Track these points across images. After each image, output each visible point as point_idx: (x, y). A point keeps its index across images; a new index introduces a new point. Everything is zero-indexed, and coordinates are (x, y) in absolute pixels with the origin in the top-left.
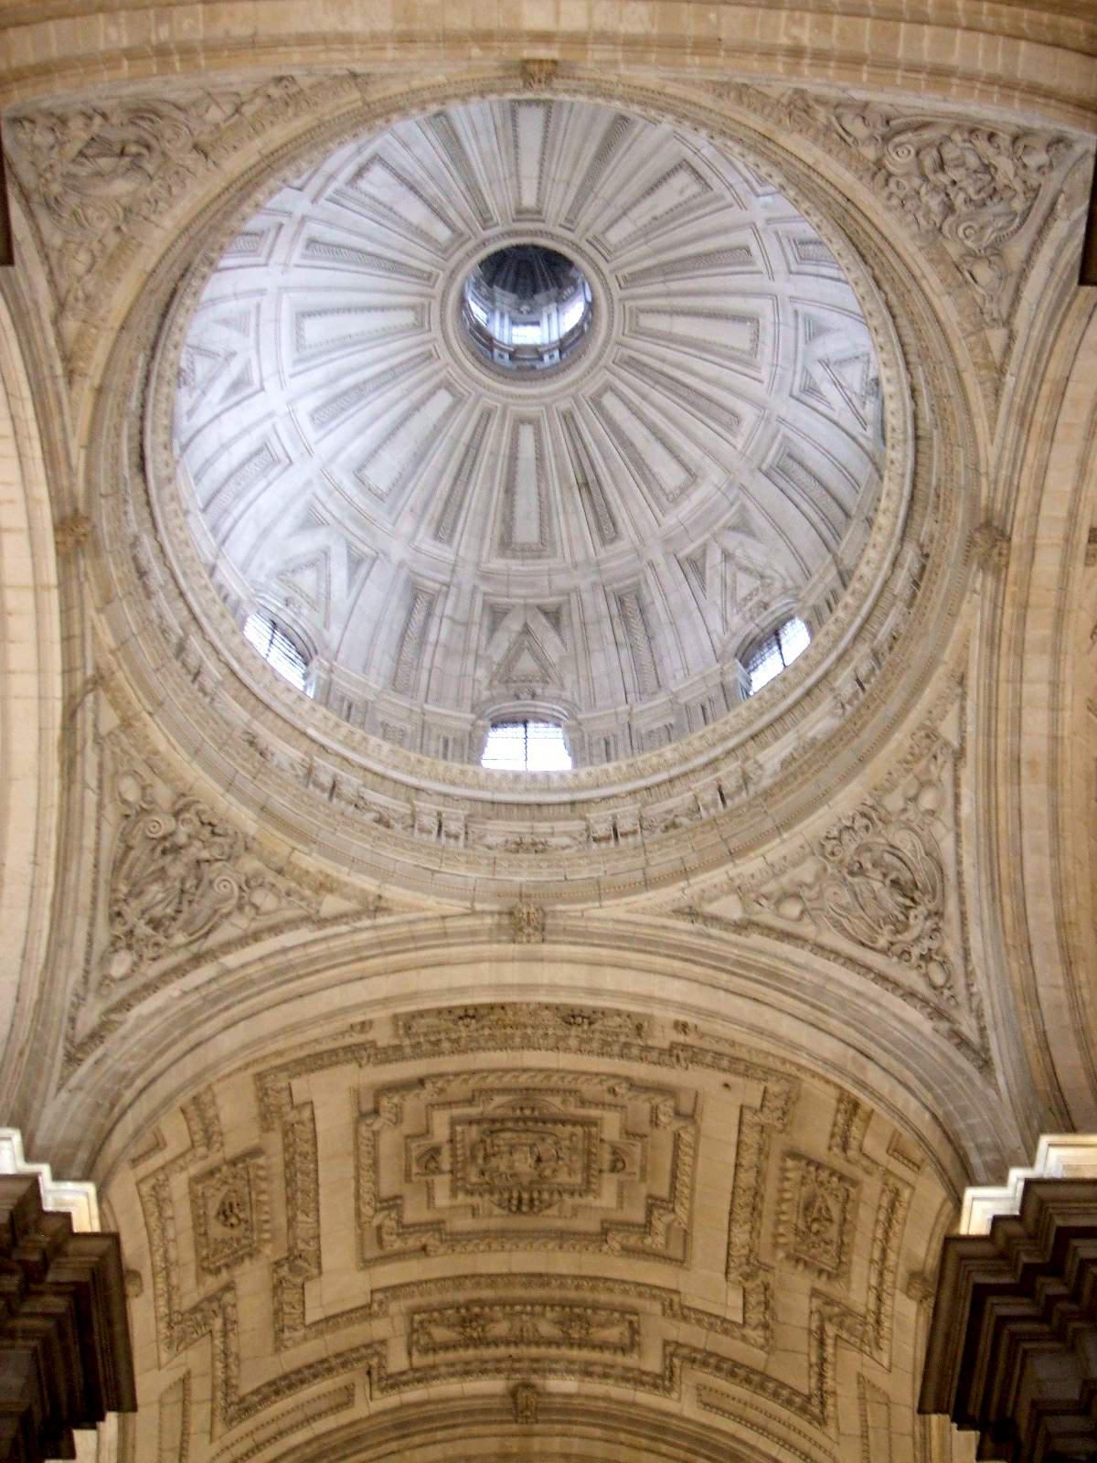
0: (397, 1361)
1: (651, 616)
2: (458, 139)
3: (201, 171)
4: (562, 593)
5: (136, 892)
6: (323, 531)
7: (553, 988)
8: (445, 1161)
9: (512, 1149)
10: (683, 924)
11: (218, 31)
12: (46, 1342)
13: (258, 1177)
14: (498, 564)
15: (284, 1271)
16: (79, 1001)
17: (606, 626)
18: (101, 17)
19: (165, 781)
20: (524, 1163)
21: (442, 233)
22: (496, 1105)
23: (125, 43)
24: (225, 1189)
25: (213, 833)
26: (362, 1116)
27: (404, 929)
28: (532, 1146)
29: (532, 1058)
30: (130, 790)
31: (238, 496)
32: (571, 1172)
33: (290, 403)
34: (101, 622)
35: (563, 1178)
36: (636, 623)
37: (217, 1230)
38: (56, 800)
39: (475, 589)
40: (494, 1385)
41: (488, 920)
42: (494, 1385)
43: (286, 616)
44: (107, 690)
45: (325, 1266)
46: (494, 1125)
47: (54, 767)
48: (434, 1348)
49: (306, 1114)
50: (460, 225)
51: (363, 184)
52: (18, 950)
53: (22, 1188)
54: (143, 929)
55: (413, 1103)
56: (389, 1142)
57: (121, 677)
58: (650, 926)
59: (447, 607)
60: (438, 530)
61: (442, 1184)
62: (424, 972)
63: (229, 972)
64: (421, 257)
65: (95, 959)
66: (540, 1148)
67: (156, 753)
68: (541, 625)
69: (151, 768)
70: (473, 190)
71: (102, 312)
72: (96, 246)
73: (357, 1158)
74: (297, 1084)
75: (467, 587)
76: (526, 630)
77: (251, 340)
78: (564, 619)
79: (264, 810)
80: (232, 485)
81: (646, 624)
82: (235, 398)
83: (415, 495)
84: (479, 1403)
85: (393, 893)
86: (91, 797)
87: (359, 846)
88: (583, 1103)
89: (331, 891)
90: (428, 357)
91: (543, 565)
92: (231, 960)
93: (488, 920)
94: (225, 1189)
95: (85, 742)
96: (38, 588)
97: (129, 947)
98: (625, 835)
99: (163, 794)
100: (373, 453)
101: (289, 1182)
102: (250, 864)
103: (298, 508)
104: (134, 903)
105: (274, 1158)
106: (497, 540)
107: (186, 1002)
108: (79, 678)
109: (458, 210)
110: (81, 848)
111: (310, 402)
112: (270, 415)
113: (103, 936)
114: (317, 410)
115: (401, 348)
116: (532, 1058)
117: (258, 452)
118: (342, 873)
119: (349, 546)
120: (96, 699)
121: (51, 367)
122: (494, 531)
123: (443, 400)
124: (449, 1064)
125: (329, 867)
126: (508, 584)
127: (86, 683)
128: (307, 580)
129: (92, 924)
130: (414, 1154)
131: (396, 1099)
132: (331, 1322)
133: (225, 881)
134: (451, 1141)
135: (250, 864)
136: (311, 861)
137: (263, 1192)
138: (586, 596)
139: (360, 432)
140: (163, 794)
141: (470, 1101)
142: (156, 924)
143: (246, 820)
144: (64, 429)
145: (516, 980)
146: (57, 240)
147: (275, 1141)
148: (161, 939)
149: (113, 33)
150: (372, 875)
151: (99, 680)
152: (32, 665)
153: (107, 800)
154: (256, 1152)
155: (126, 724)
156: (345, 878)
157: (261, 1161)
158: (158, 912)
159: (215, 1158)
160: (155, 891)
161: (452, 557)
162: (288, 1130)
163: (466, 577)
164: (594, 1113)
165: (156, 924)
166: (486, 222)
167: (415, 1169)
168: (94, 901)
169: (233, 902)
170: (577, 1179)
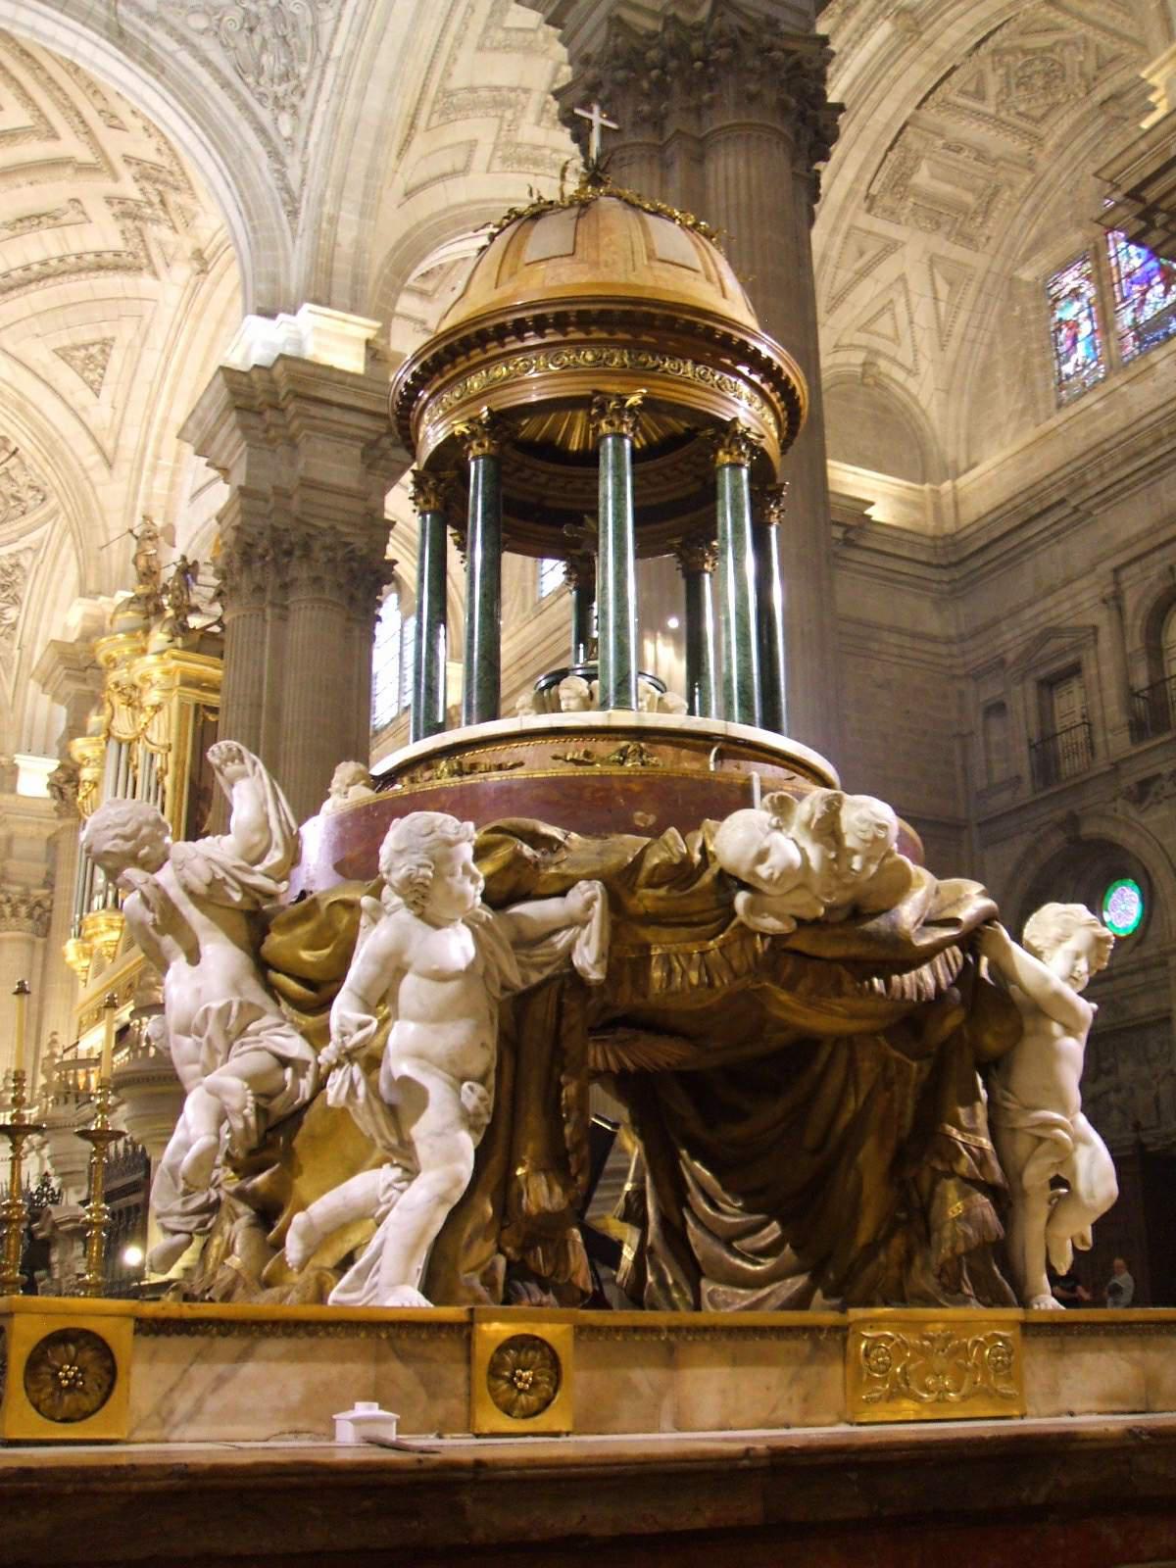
5: (260, 71)
40: (883, 31)
42: (883, 31)
53: (221, 378)
54: (280, 90)
84: (884, 52)
95: (147, 35)
142: (285, 77)
160: (267, 60)
165: (285, 77)
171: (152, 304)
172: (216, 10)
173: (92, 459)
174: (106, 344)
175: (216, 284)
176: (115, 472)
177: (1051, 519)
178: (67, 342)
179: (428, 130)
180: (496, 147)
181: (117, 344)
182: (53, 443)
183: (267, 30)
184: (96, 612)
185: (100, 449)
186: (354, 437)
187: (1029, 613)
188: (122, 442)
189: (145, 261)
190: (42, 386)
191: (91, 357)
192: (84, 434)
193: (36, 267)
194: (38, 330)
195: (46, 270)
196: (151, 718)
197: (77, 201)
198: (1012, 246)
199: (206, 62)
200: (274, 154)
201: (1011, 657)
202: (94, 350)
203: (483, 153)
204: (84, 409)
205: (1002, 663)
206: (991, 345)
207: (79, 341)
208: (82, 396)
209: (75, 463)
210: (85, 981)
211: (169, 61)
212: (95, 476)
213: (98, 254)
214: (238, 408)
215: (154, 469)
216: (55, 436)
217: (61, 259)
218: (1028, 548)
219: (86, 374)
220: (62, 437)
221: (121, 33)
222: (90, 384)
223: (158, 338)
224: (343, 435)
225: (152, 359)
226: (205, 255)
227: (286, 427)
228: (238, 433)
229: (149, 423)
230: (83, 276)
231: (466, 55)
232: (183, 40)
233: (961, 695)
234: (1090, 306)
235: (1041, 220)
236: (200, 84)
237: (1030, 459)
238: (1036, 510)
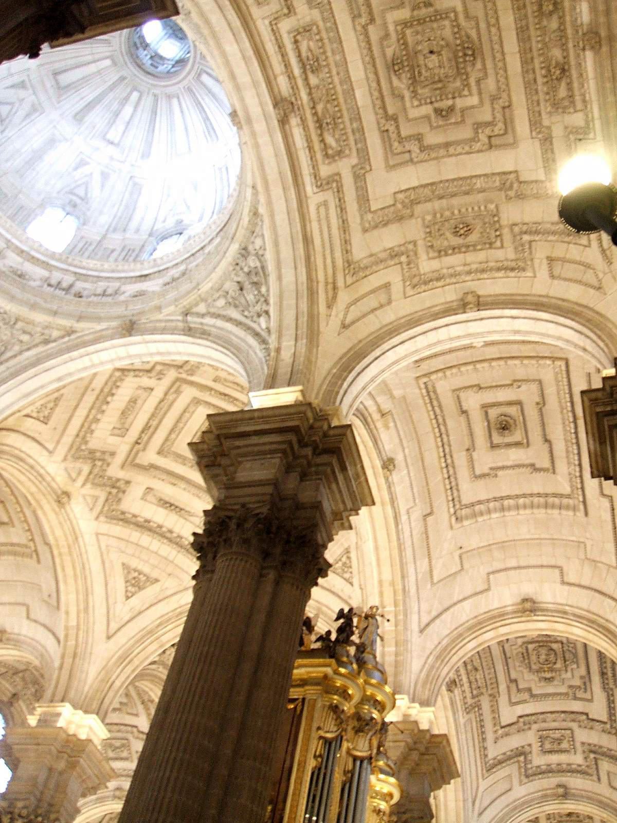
2: (89, 104)
7: (261, 104)
13: (442, 216)
15: (512, 193)
21: (135, 95)
28: (425, 57)
32: (442, 28)
34: (165, 311)
35: (448, 33)
37: (473, 237)
44: (191, 308)
45: (511, 169)
46: (414, 81)
48: (571, 96)
50: (128, 90)
51: (116, 141)
56: (433, 138)
61: (460, 103)
64: (147, 102)
66: (426, 51)
67: (212, 288)
69: (219, 289)
70: (112, 88)
73: (443, 157)
86: (219, 323)
88: (387, 36)
89: (257, 209)
90: (189, 90)
101: (454, 195)
109: (120, 91)
115: (187, 101)
116: (357, 71)
121: (65, 343)
123: (205, 78)
124: (369, 119)
125: (246, 211)
130: (441, 123)
134: (431, 103)
137: (453, 213)
146: (17, 348)
147: (418, 209)
153: (224, 313)
155: (203, 300)
156: (249, 204)
162: (415, 202)
166: (122, 79)
167: (453, 120)
179: (347, 287)
180: (404, 281)
186: (272, 452)
190: (327, 593)
199: (230, 320)
203: (397, 287)
221: (190, 329)
224: (264, 453)
231: (356, 237)
232: (218, 316)
236: (227, 331)
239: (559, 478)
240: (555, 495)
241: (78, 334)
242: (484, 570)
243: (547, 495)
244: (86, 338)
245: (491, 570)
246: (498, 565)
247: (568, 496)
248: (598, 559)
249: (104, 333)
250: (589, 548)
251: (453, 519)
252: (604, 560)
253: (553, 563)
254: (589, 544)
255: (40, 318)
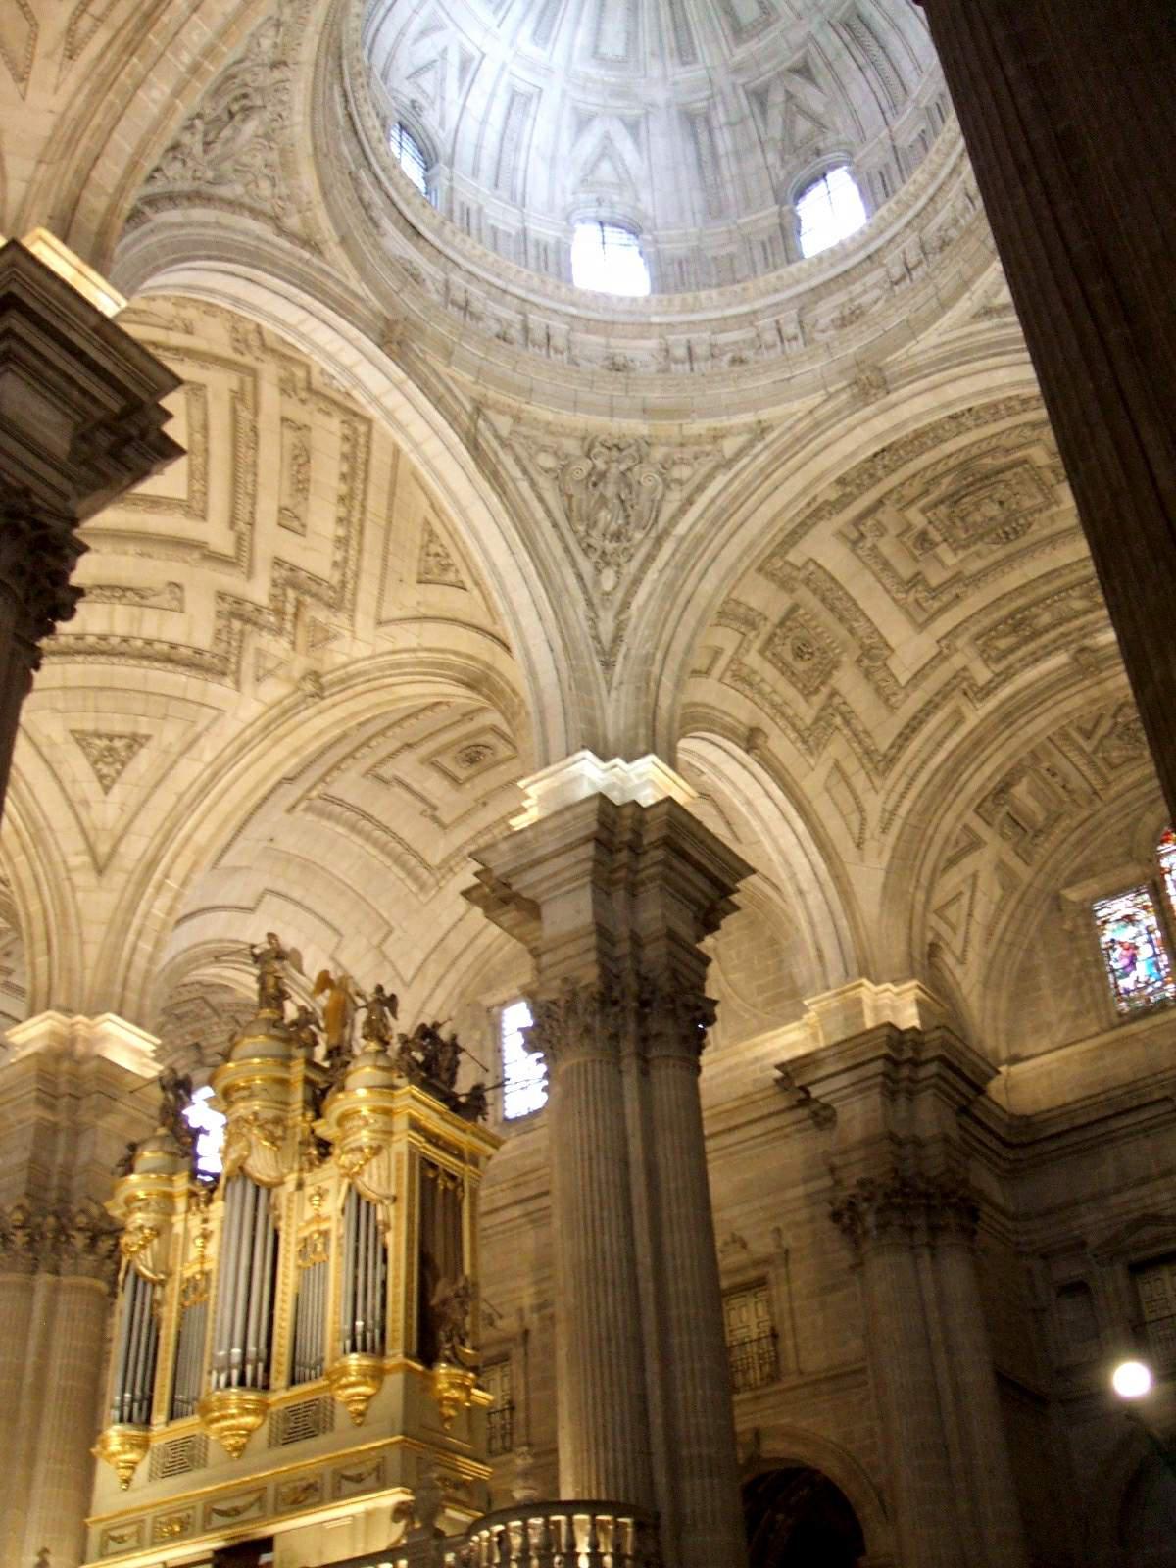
0: (982, 674)
1: (874, 26)
3: (290, 75)
4: (803, 45)
5: (592, 524)
6: (596, 123)
7: (917, 417)
8: (936, 536)
9: (977, 505)
10: (985, 325)
11: (218, 20)
12: (666, 879)
14: (741, 53)
15: (866, 662)
16: (594, 622)
17: (846, 55)
18: (140, 93)
19: (569, 436)
20: (992, 509)
22: (945, 486)
23: (167, 90)
24: (788, 641)
25: (620, 450)
26: (854, 543)
27: (787, 438)
29: (949, 447)
30: (547, 461)
31: (517, 149)
32: (1032, 496)
33: (512, 44)
34: (455, 371)
35: (1027, 503)
36: (869, 40)
37: (800, 666)
38: (500, 506)
39: (734, 86)
40: (1060, 659)
41: (844, 397)
42: (1060, 659)
43: (604, 213)
45: (892, 642)
46: (953, 499)
47: (485, 486)
48: (1004, 654)
49: (812, 567)
52: (535, 618)
53: (595, 803)
54: (610, 546)
55: (887, 515)
56: (887, 547)
57: (492, 394)
58: (960, 338)
59: (720, 117)
60: (681, 55)
61: (941, 548)
62: (819, 458)
63: (683, 539)
65: (589, 584)
66: (997, 496)
67: (548, 424)
68: (799, 85)
69: (552, 433)
71: (304, 199)
72: (266, 171)
74: (791, 557)
75: (728, 90)
76: (790, 97)
77: (452, 28)
78: (814, 70)
79: (646, 412)
80: (508, 146)
81: (876, 39)
82: (469, 79)
83: (646, 42)
84: (1054, 677)
85: (766, 414)
86: (524, 486)
87: (724, 393)
88: (1008, 451)
89: (723, 437)
91: (773, 33)
92: (681, 529)
93: (844, 397)
94: (788, 641)
95: (496, 454)
96: (398, 386)
97: (608, 564)
98: (915, 267)
99: (572, 446)
100: (598, 32)
101: (832, 609)
102: (658, 453)
103: (567, 119)
104: (594, 533)
105: (813, 602)
106: (728, 32)
107: (664, 579)
108: (464, 418)
110: (537, 523)
111: (527, 29)
112: (503, 67)
113: (586, 566)
114: (535, 33)
117: (512, 101)
118: (725, 422)
119: (622, 119)
120: (486, 420)
122: (722, 26)
124: (894, 479)
126: (758, 64)
127: (471, 417)
128: (605, 169)
129: (574, 564)
130: (910, 544)
131: (870, 522)
132: (919, 676)
133: (647, 477)
135: (658, 453)
136: (698, 427)
138: (821, 38)
139: (578, 21)
140: (572, 446)
141: (926, 492)
142: (617, 536)
143: (638, 427)
144: (338, 282)
145: (887, 426)
146: (239, 190)
147: (804, 594)
148: (626, 544)
149: (155, 94)
150: (746, 410)
151: (479, 408)
152: (427, 431)
154: (794, 608)
155: (517, 419)
157: (801, 611)
158: (613, 527)
159: (766, 629)
160: (604, 516)
161: (703, 72)
162: (807, 582)
163: (723, 80)
164: (1019, 454)
165: (617, 536)
168: (567, 549)
169: (660, 488)
170: (1039, 499)
171: (213, 712)
172: (567, 456)
173: (81, 861)
174: (136, 741)
175: (321, 712)
176: (105, 881)
177: (1143, 1115)
178: (89, 726)
181: (152, 744)
182: (39, 830)
183: (610, 491)
184: (65, 1031)
185: (91, 849)
186: (692, 900)
187: (1114, 1200)
188: (122, 848)
189: (233, 667)
190: (42, 766)
191: (110, 749)
192: (76, 829)
193: (91, 640)
194: (60, 705)
195: (103, 645)
196: (367, 1160)
197: (177, 585)
198: (1055, 870)
199: (541, 499)
200: (590, 603)
201: (1093, 1240)
202: (118, 744)
204: (86, 803)
205: (1083, 1244)
206: (1030, 951)
207: (104, 728)
208: (90, 787)
209: (57, 858)
210: (127, 1481)
211: (510, 486)
212: (80, 879)
213: (173, 646)
214: (598, 841)
215: (159, 887)
216: (42, 823)
217: (125, 640)
218: (1110, 1139)
219: (100, 766)
220: (49, 827)
222: (101, 777)
223: (208, 749)
225: (189, 772)
226: (324, 680)
227: (637, 872)
228: (589, 865)
229: (168, 837)
230: (145, 663)
233: (1029, 1272)
234: (1149, 933)
235: (1087, 852)
237: (1101, 1058)
238: (1135, 1103)
239: (442, 843)
240: (416, 854)
241: (315, 260)
242: (266, 882)
243: (408, 848)
244: (330, 284)
245: (270, 886)
246: (280, 886)
247: (428, 867)
248: (393, 958)
249: (358, 305)
250: (392, 938)
251: (303, 805)
252: (400, 965)
253: (337, 923)
254: (397, 933)
255: (307, 179)
